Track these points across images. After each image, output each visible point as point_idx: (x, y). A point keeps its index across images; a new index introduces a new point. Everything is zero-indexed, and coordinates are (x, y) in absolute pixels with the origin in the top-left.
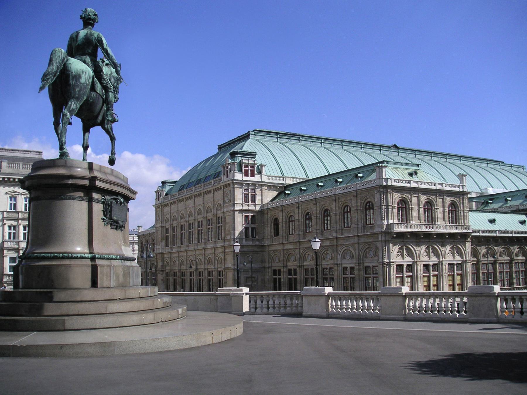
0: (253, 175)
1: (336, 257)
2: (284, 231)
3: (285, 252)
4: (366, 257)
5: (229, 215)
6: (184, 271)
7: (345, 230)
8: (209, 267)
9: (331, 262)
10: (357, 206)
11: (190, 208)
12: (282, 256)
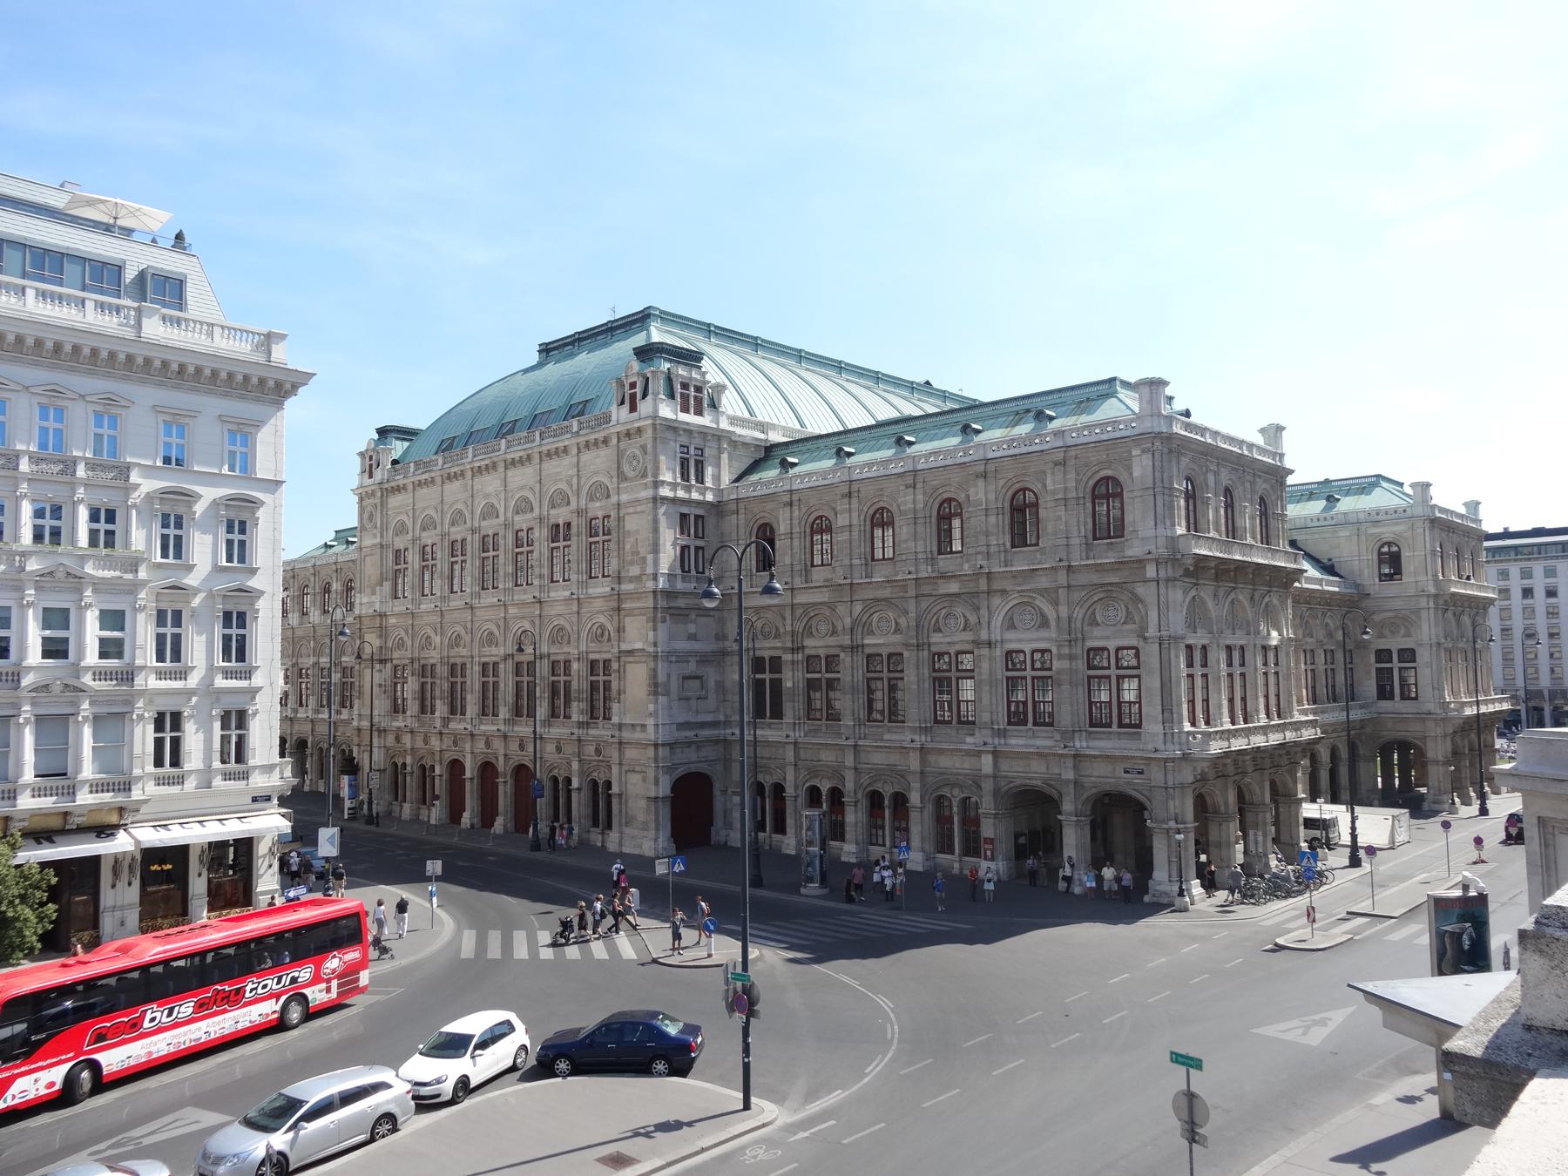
0: (699, 412)
1: (985, 625)
2: (797, 557)
3: (799, 612)
4: (1094, 623)
5: (636, 513)
6: (459, 661)
7: (1015, 553)
8: (552, 651)
9: (969, 636)
10: (1066, 490)
11: (487, 496)
12: (788, 622)
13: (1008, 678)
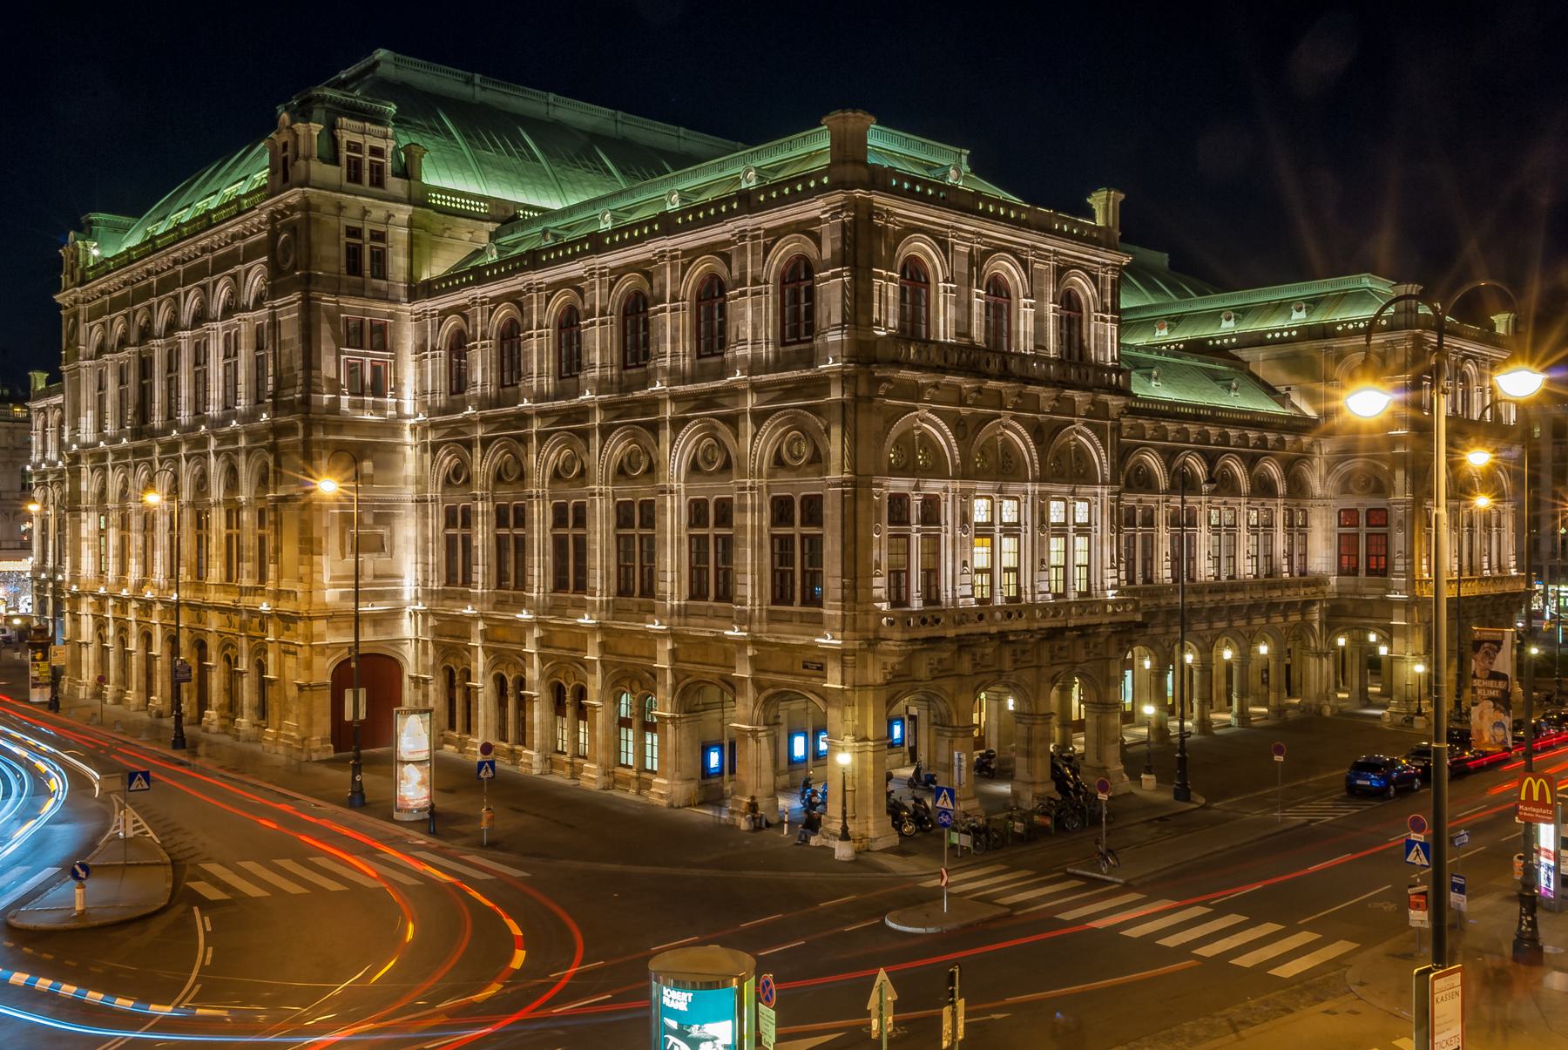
13: (691, 537)
